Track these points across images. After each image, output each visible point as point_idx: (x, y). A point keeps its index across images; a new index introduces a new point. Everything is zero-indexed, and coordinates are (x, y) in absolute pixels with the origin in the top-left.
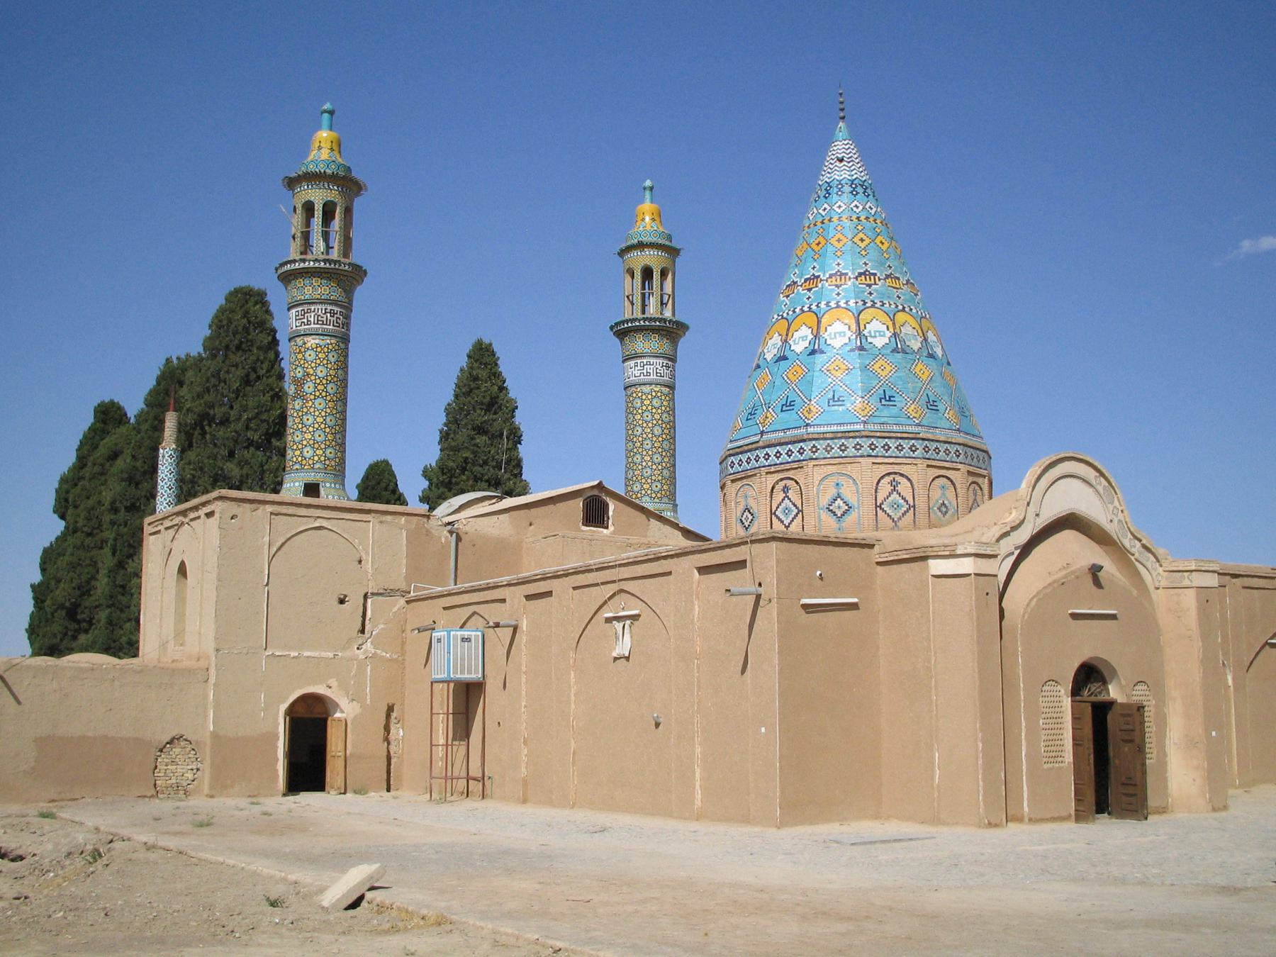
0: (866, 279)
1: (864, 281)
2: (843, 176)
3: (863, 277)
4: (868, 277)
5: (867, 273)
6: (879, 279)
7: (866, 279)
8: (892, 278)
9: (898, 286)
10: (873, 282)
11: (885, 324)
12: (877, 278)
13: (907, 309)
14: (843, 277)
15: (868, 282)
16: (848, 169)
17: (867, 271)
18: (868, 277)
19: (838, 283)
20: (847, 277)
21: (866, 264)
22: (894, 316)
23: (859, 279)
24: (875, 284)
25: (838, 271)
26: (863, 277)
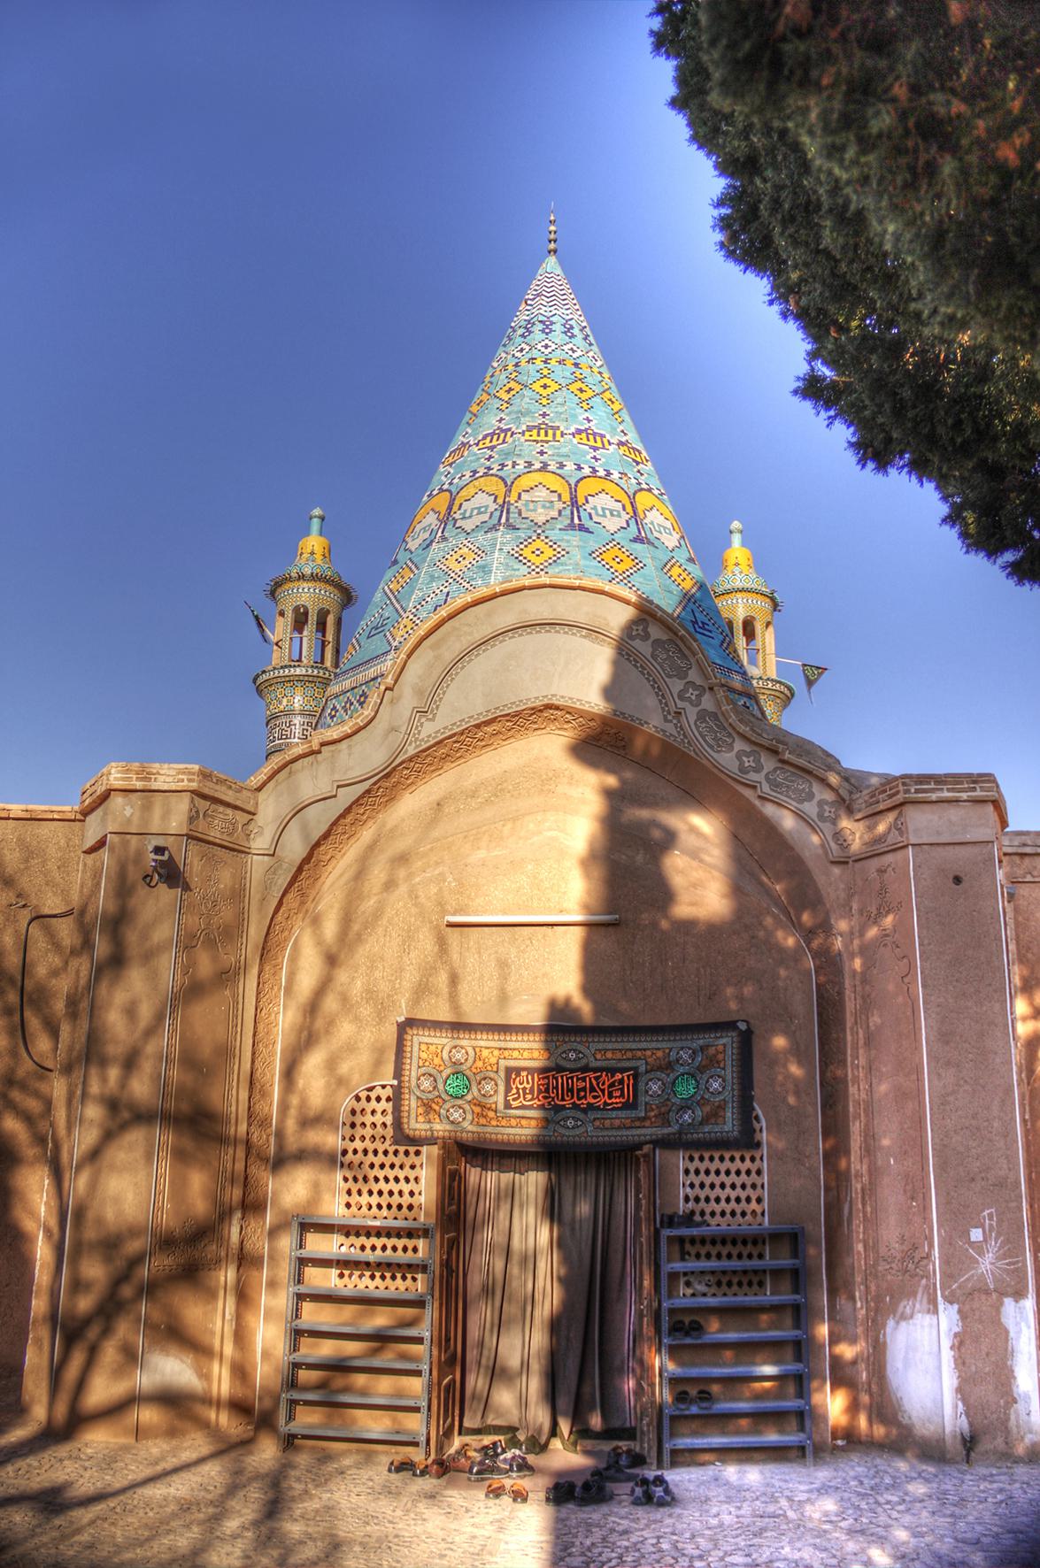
0: (539, 435)
1: (535, 437)
2: (571, 316)
3: (535, 432)
4: (542, 432)
5: (543, 426)
6: (562, 435)
7: (539, 435)
8: (588, 434)
9: (599, 445)
10: (550, 437)
11: (619, 501)
12: (558, 433)
13: (602, 473)
14: (502, 435)
15: (542, 437)
16: (545, 304)
17: (589, 428)
18: (542, 432)
19: (494, 443)
20: (509, 434)
21: (589, 421)
22: (576, 486)
23: (527, 434)
24: (604, 448)
25: (499, 428)
26: (535, 432)
